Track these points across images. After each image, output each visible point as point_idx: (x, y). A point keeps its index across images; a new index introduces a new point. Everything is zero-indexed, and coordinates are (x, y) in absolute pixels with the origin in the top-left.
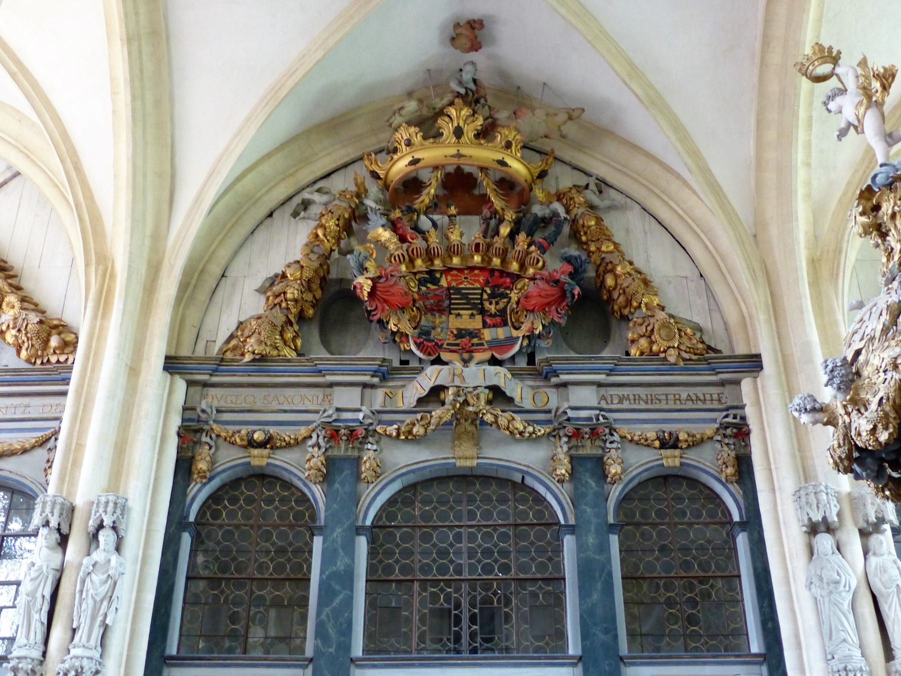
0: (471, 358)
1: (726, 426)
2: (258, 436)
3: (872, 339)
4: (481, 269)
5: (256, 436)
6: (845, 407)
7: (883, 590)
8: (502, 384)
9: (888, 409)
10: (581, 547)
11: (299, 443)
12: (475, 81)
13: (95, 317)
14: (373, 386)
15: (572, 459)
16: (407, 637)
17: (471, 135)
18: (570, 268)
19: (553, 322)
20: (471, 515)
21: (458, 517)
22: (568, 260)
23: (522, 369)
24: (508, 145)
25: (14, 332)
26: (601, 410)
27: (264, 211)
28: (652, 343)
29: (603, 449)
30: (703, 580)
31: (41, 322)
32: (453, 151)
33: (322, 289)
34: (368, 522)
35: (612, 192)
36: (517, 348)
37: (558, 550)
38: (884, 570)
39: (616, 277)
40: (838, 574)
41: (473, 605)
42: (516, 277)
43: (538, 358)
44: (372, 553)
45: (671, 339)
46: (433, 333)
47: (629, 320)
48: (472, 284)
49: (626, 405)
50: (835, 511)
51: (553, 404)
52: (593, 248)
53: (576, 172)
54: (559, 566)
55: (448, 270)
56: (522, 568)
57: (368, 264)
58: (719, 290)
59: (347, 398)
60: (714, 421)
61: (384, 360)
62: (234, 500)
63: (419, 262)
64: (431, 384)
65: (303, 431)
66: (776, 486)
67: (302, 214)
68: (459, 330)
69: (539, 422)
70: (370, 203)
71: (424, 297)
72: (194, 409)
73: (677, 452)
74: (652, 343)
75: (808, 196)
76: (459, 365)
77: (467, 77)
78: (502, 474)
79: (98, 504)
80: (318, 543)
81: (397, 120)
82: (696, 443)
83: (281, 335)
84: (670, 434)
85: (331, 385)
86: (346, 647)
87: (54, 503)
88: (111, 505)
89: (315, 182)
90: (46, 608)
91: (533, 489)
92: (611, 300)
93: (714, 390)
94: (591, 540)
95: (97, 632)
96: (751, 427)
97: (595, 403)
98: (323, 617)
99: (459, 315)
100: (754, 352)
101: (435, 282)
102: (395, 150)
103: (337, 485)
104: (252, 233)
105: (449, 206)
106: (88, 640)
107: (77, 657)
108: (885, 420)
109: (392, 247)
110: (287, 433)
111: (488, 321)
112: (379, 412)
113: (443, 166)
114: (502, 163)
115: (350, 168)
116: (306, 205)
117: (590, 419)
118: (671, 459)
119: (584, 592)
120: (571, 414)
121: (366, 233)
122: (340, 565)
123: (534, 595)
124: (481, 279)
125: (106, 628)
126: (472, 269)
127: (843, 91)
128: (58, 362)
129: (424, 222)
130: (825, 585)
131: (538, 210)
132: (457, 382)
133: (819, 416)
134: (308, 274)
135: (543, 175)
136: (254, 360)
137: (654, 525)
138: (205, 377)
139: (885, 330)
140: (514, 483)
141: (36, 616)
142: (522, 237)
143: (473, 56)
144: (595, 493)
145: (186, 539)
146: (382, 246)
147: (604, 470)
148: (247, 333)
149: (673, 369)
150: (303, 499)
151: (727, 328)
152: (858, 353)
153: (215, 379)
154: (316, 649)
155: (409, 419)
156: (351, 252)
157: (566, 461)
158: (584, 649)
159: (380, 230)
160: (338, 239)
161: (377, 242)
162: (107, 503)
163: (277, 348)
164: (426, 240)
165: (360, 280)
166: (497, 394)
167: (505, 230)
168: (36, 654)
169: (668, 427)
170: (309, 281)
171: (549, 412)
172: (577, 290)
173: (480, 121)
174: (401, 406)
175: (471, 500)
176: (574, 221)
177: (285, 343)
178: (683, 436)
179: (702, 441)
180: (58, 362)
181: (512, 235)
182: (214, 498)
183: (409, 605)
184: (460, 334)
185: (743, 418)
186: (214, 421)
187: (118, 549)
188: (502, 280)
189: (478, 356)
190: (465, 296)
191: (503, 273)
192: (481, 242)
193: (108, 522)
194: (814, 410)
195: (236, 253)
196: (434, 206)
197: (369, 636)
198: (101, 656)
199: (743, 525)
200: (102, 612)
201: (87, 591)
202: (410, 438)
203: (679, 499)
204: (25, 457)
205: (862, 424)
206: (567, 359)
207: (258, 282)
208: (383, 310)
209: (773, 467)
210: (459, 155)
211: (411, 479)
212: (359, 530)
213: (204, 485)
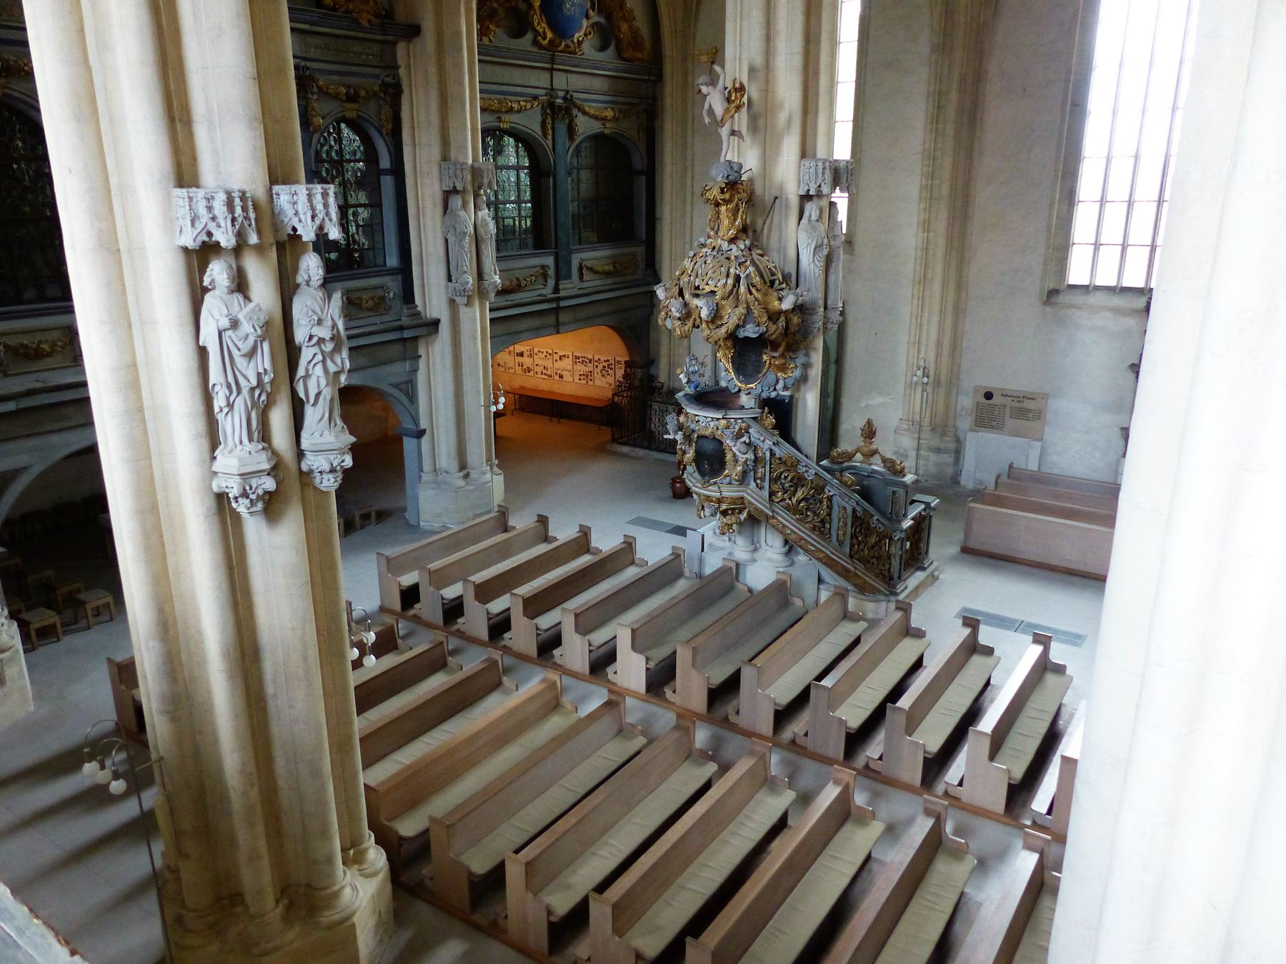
60: (377, 77)
66: (417, 142)
73: (356, 106)
96: (404, 88)
169: (353, 80)
209: (416, 125)
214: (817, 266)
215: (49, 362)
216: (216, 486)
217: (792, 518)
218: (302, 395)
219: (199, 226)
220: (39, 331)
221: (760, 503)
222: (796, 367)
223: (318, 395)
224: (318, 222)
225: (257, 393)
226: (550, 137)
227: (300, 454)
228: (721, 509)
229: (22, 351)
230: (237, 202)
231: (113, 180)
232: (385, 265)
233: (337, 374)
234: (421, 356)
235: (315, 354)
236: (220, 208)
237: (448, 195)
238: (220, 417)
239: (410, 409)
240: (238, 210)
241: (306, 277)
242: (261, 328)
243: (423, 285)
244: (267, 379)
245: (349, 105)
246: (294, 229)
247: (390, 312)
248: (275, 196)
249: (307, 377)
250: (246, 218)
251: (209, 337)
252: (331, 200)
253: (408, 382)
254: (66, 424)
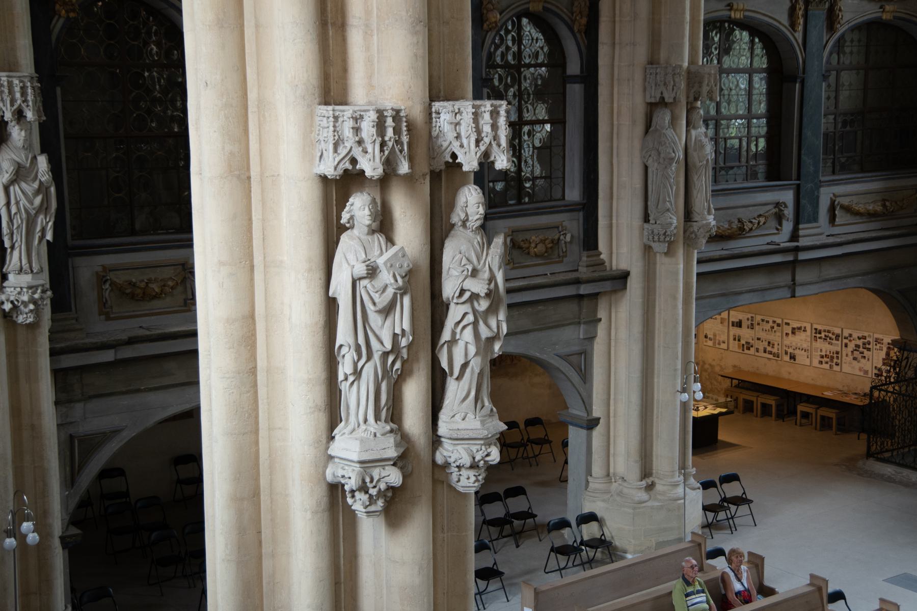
40: (674, 152)
66: (617, 41)
130: (661, 161)
200: (39, 228)
201: (17, 203)
209: (617, 19)
215: (157, 304)
216: (332, 473)
218: (444, 364)
219: (343, 151)
220: (150, 267)
223: (465, 366)
224: (483, 148)
225: (391, 359)
226: (800, 28)
227: (436, 441)
229: (128, 291)
230: (389, 122)
231: (252, 96)
232: (564, 198)
233: (491, 340)
234: (600, 320)
235: (465, 314)
236: (368, 129)
237: (652, 108)
238: (344, 386)
239: (581, 390)
240: (390, 133)
241: (463, 216)
242: (403, 277)
243: (610, 226)
244: (404, 342)
246: (454, 156)
247: (565, 259)
248: (434, 115)
249: (453, 341)
250: (398, 142)
251: (341, 287)
252: (502, 121)
253: (581, 354)
254: (166, 381)
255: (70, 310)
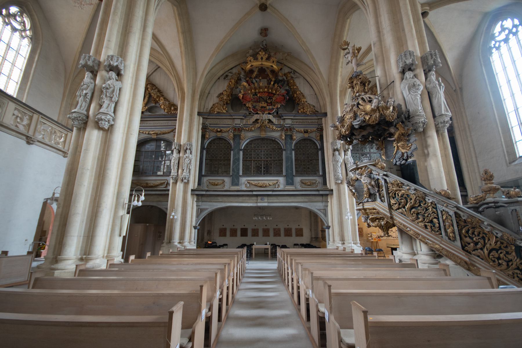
0: (264, 113)
1: (318, 128)
2: (219, 130)
3: (348, 112)
4: (267, 92)
5: (218, 130)
6: (340, 126)
7: (347, 163)
8: (271, 119)
9: (348, 127)
10: (286, 153)
11: (228, 131)
12: (266, 45)
13: (181, 103)
14: (243, 119)
15: (285, 135)
16: (251, 171)
17: (265, 59)
18: (287, 92)
19: (282, 105)
20: (264, 147)
21: (261, 147)
22: (286, 90)
23: (275, 115)
24: (273, 62)
25: (163, 106)
26: (292, 124)
27: (217, 77)
28: (304, 110)
29: (292, 133)
30: (311, 160)
31: (169, 104)
32: (260, 63)
33: (231, 96)
34: (242, 148)
35: (297, 73)
36: (274, 110)
37: (282, 154)
38: (348, 158)
39: (297, 94)
41: (264, 165)
42: (274, 94)
43: (279, 113)
44: (243, 155)
45: (308, 109)
46: (256, 107)
47: (299, 104)
48: (265, 96)
49: (297, 124)
50: (339, 146)
51: (282, 123)
52: (292, 88)
53: (289, 68)
54: (282, 157)
55: (259, 92)
56: (274, 158)
57: (241, 91)
58: (319, 98)
59: (238, 122)
61: (245, 113)
62: (214, 143)
63: (253, 90)
64: (256, 119)
65: (228, 129)
67: (226, 79)
68: (262, 106)
69: (279, 127)
70: (242, 76)
71: (254, 98)
72: (204, 124)
73: (307, 134)
74: (304, 110)
75: (341, 75)
76: (262, 114)
77: (264, 44)
78: (270, 138)
79: (186, 144)
80: (232, 152)
81: (248, 55)
82: (311, 132)
83: (223, 107)
84: (306, 130)
85: (234, 119)
86: (238, 173)
87: (177, 144)
88: (189, 145)
89: (229, 70)
90: (177, 165)
91: (277, 141)
92: (295, 100)
93: (317, 121)
94: (289, 152)
95: (188, 170)
97: (291, 123)
98: (234, 167)
99: (262, 103)
100: (326, 112)
101: (257, 95)
102: (247, 63)
103: (236, 140)
104: (215, 83)
105: (259, 77)
106: (186, 171)
107: (184, 175)
108: (348, 129)
109: (247, 87)
110: (224, 129)
111: (268, 104)
112: (244, 125)
113: (258, 67)
114: (272, 66)
115: (237, 67)
116: (227, 76)
117: (289, 127)
118: (306, 135)
119: (287, 162)
120: (285, 125)
121: (241, 83)
122: (237, 157)
123: (277, 163)
124: (267, 95)
125: (190, 169)
126: (265, 92)
127: (348, 53)
128: (174, 113)
129: (254, 81)
131: (280, 78)
132: (261, 118)
133: (335, 128)
134: (228, 93)
135: (281, 69)
136: (217, 113)
137: (302, 149)
138: (207, 117)
139: (350, 110)
140: (273, 140)
141: (175, 167)
142: (276, 85)
143: (266, 38)
144: (290, 143)
145: (205, 152)
146: (245, 87)
147: (292, 138)
148: (215, 107)
149: (308, 115)
150: (229, 143)
151: (320, 107)
152: (344, 115)
153: (209, 117)
154: (233, 174)
155: (251, 126)
156: (238, 88)
157: (284, 136)
158: (286, 174)
159: (244, 83)
160: (235, 85)
161: (243, 85)
162: (188, 144)
163: (222, 110)
164: (255, 85)
165: (240, 95)
166: (270, 121)
167: (272, 83)
168: (176, 174)
169: (306, 128)
170: (228, 95)
171: (281, 125)
172: (288, 98)
173: (267, 56)
174: (249, 123)
175: (264, 144)
176: (288, 81)
177: (224, 109)
178: (309, 130)
179: (313, 131)
180: (174, 113)
181: (274, 84)
182: (210, 143)
183: (251, 165)
184: (262, 107)
185: (322, 127)
186: (209, 127)
187: (191, 153)
188: (271, 95)
189: (266, 112)
190: (263, 99)
191: (272, 93)
192: (267, 85)
193: (188, 148)
194: (334, 127)
195: (212, 87)
196: (256, 77)
197: (243, 171)
198: (189, 175)
199: (320, 149)
202: (251, 131)
203: (307, 144)
204: (169, 134)
205: (343, 130)
206: (285, 113)
207: (217, 95)
208: (245, 102)
210: (262, 64)
211: (251, 139)
212: (241, 150)
213: (208, 140)
214: (412, 94)
217: (408, 220)
221: (383, 210)
222: (412, 145)
228: (370, 218)
243: (330, 180)
245: (305, 134)
253: (324, 210)
255: (201, 185)
